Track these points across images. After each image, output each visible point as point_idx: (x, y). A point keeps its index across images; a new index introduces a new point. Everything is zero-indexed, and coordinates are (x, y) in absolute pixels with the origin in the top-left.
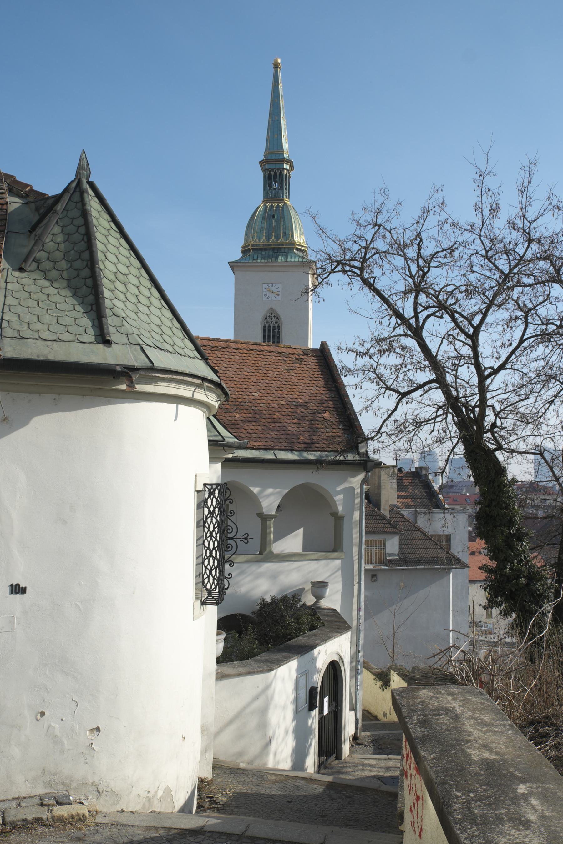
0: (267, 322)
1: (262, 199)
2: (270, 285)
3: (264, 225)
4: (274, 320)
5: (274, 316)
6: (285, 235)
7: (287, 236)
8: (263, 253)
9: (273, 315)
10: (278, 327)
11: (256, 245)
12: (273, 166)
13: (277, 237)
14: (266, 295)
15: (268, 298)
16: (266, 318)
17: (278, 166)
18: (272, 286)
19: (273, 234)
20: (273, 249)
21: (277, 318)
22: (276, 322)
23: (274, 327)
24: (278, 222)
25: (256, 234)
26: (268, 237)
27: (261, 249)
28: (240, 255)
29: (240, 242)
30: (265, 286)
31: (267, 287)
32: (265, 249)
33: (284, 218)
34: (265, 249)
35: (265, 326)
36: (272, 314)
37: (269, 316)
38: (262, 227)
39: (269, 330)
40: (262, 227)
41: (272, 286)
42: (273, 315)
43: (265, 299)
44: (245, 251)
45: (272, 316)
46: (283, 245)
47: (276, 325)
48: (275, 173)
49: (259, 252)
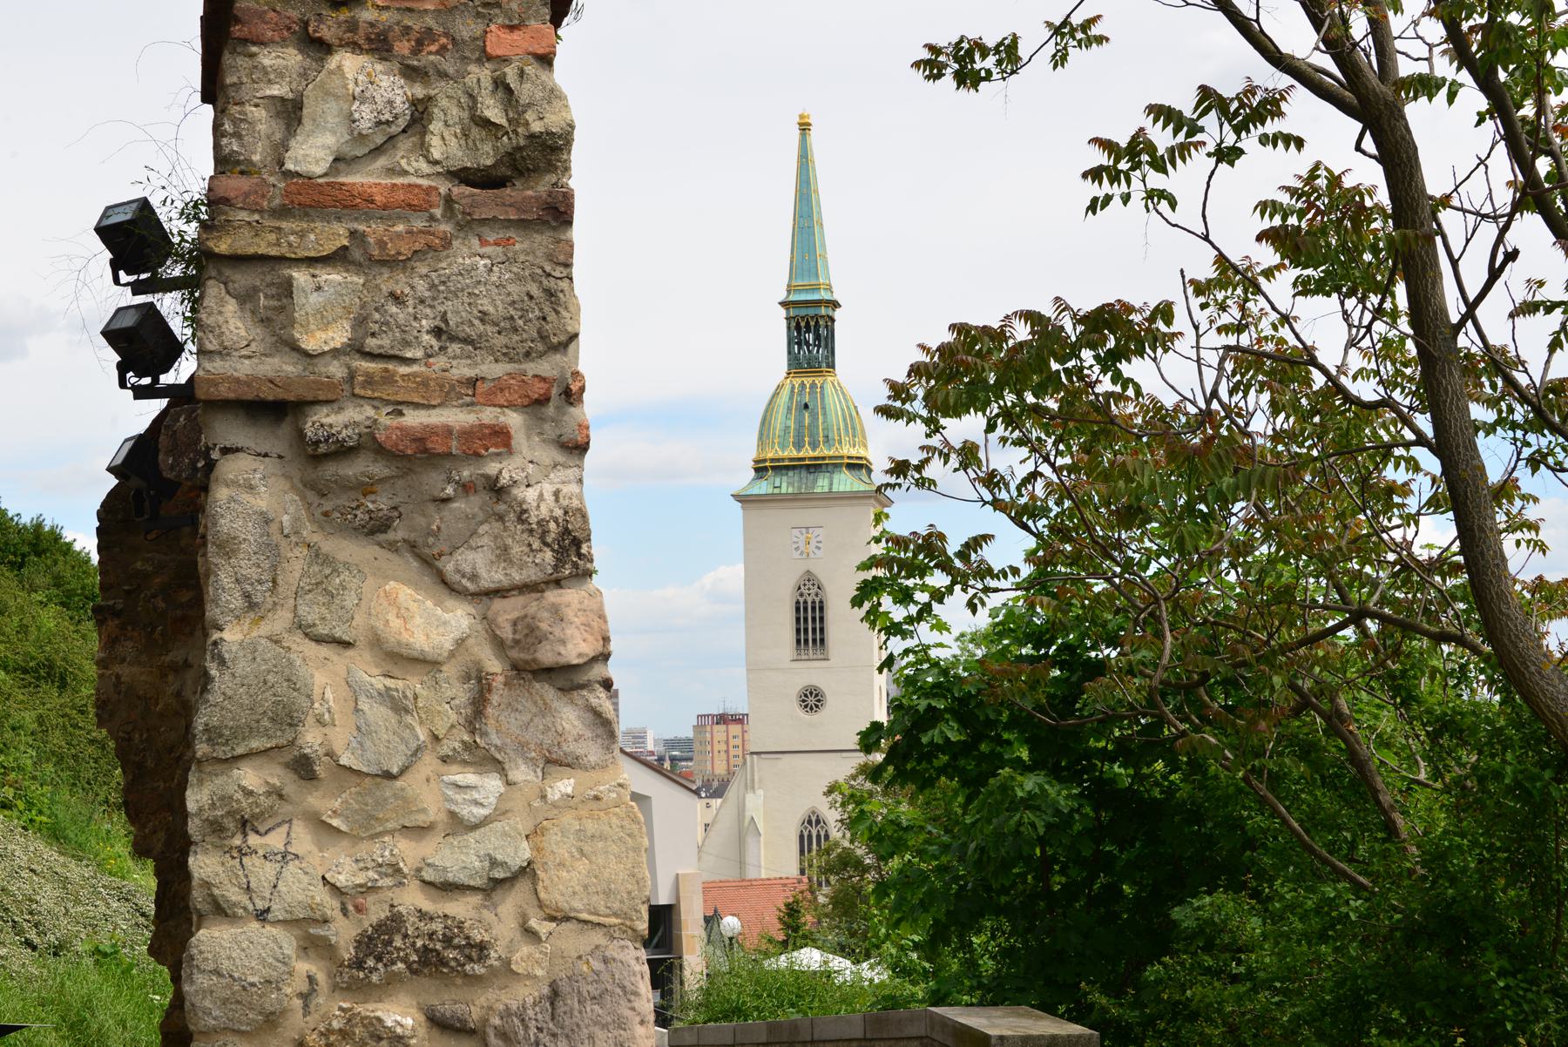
1: (785, 369)
8: (791, 473)
10: (821, 602)
11: (778, 460)
12: (803, 312)
13: (803, 385)
17: (811, 312)
24: (814, 417)
27: (787, 468)
28: (752, 473)
29: (747, 450)
30: (796, 532)
32: (794, 467)
33: (824, 408)
34: (794, 467)
35: (798, 602)
39: (806, 609)
43: (796, 555)
44: (760, 470)
45: (809, 585)
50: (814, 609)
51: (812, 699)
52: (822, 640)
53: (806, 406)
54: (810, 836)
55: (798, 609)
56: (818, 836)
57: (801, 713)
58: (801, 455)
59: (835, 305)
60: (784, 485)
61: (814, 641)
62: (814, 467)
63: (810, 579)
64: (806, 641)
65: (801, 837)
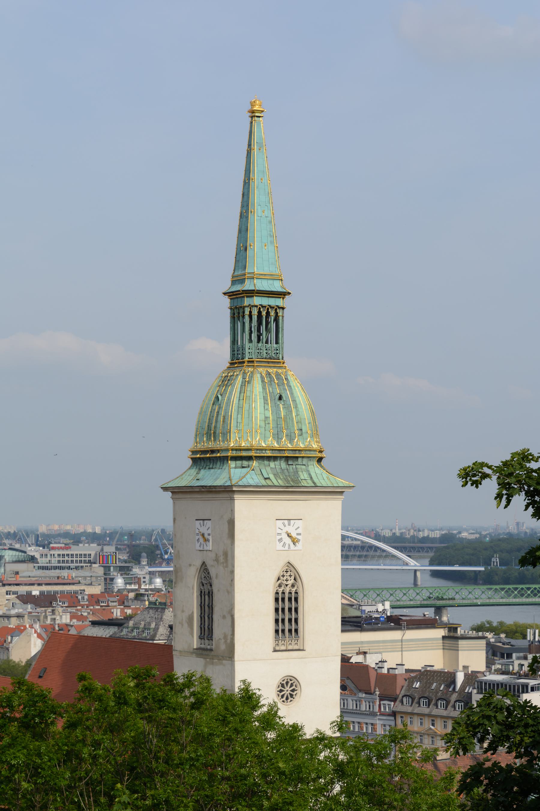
0: (280, 586)
3: (269, 414)
4: (290, 582)
5: (290, 576)
6: (301, 435)
7: (304, 435)
8: (272, 464)
9: (289, 574)
10: (296, 593)
14: (280, 540)
16: (279, 579)
18: (289, 525)
19: (285, 431)
20: (287, 458)
21: (295, 579)
22: (293, 586)
24: (288, 408)
25: (259, 431)
26: (277, 437)
27: (269, 458)
31: (282, 527)
33: (294, 401)
34: (275, 458)
35: (277, 593)
36: (287, 572)
37: (283, 576)
38: (266, 418)
39: (283, 599)
40: (266, 418)
41: (289, 525)
42: (289, 574)
43: (279, 546)
47: (294, 590)
49: (266, 462)
50: (290, 599)
52: (296, 631)
53: (280, 398)
55: (277, 600)
60: (271, 476)
62: (291, 458)
64: (283, 631)
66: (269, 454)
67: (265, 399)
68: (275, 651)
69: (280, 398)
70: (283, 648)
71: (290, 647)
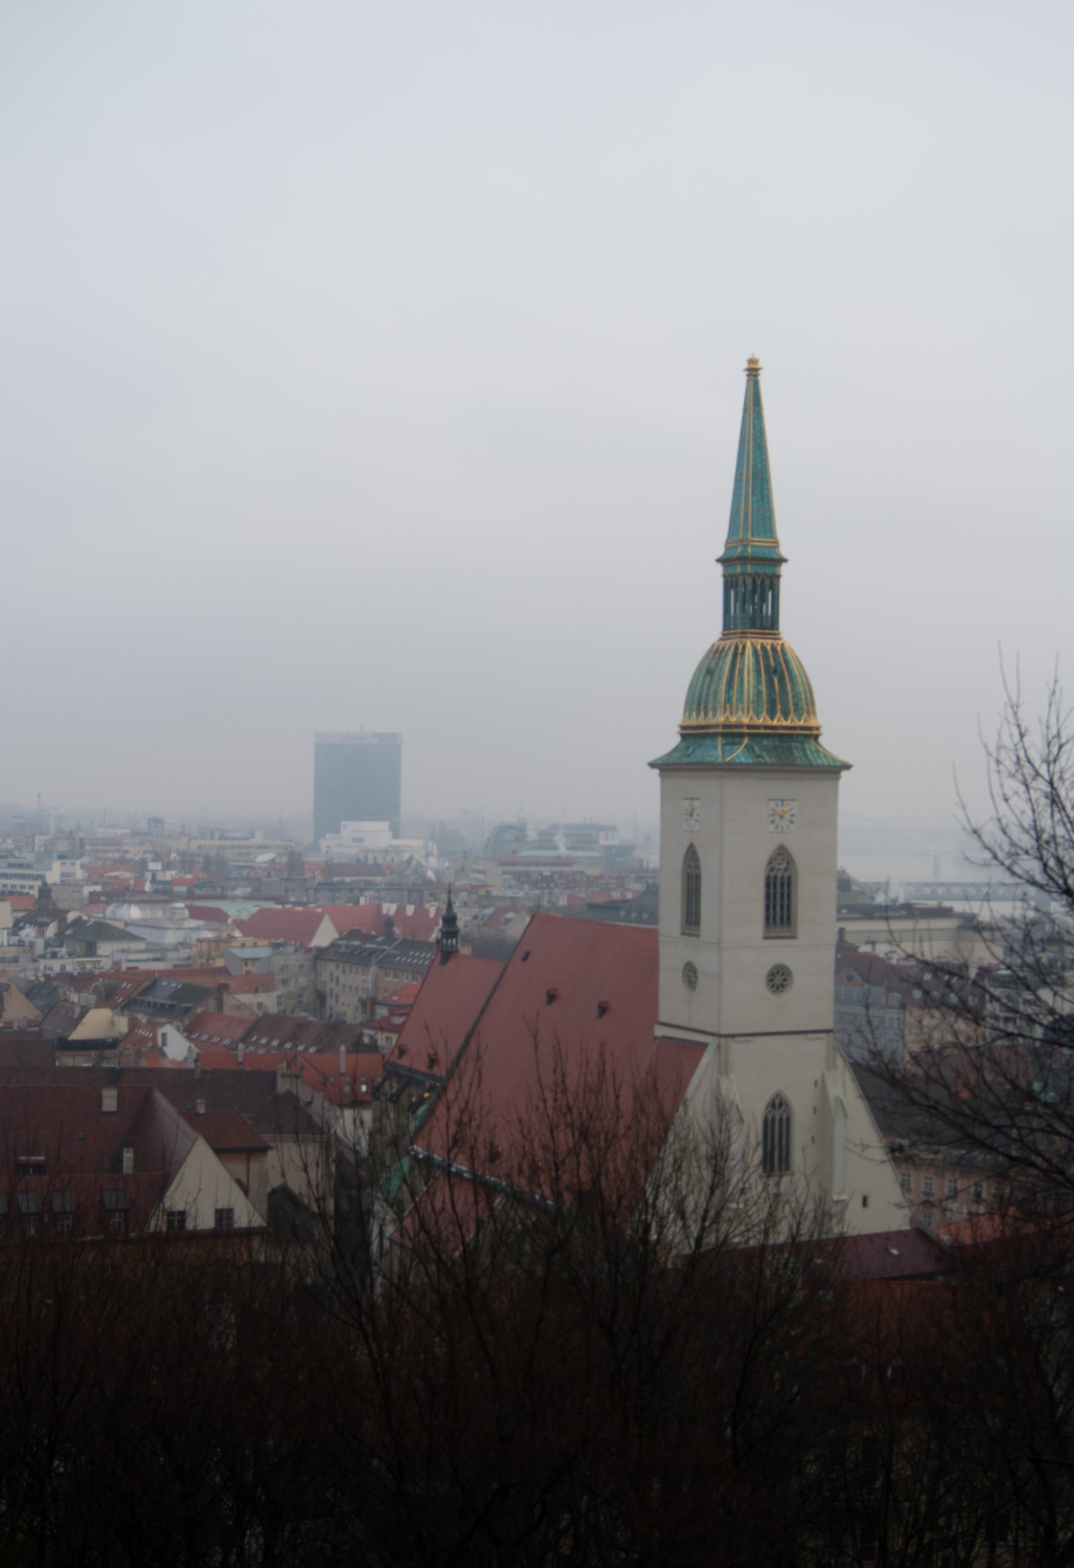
0: (772, 870)
2: (779, 803)
3: (763, 688)
10: (789, 878)
15: (777, 827)
20: (781, 736)
21: (788, 863)
22: (786, 870)
23: (783, 878)
25: (751, 706)
30: (772, 805)
43: (772, 828)
46: (794, 728)
47: (786, 874)
48: (763, 582)
51: (779, 979)
54: (773, 1120)
56: (781, 1120)
57: (767, 993)
58: (775, 722)
59: (782, 560)
61: (782, 918)
63: (782, 853)
65: (766, 1121)
66: (762, 731)
67: (758, 671)
68: (766, 938)
69: (775, 671)
70: (774, 935)
71: (782, 934)
